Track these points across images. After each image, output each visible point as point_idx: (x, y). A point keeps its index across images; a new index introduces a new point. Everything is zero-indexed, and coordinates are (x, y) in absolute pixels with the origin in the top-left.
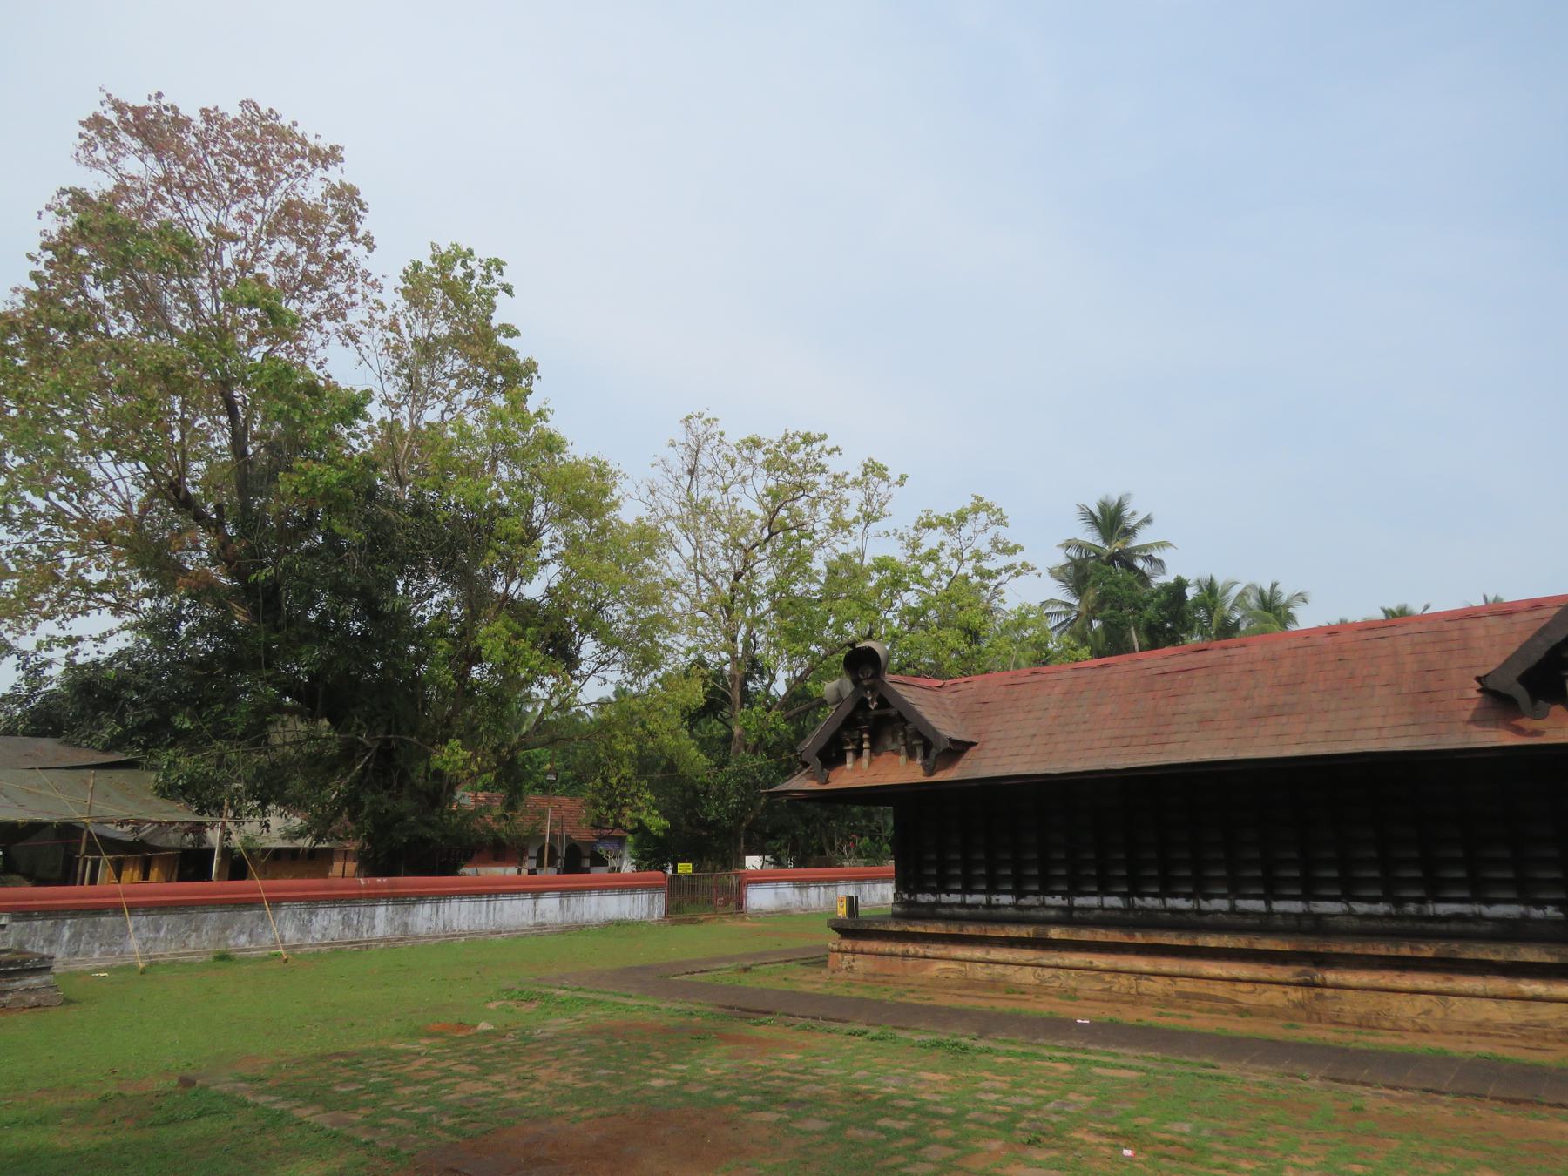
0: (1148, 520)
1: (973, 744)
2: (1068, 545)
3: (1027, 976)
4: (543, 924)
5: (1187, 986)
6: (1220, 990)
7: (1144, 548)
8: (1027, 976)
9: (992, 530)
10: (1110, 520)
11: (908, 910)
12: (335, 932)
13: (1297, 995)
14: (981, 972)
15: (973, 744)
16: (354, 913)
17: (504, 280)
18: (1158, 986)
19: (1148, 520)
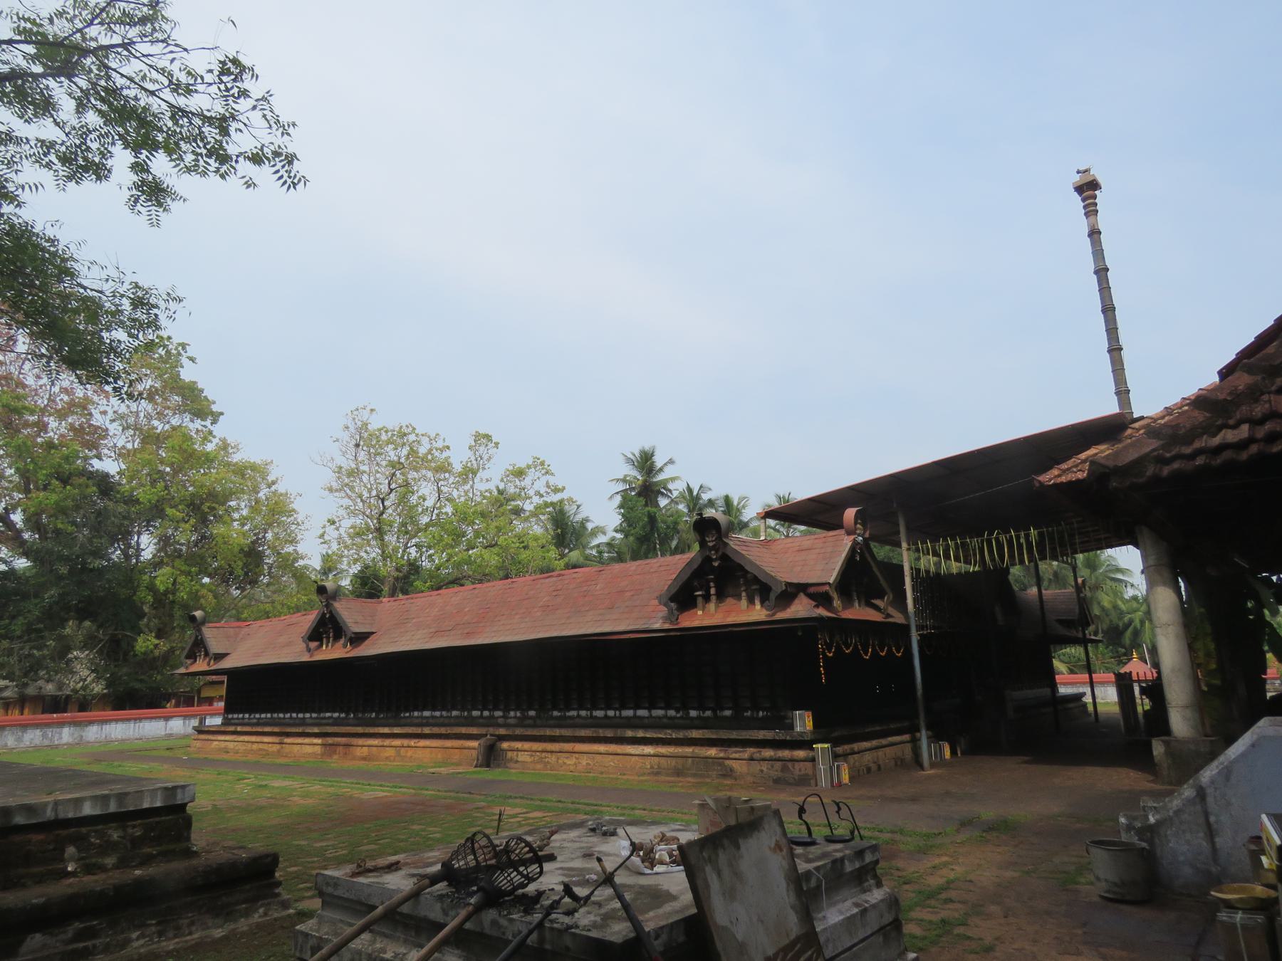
0: (671, 462)
1: (227, 654)
2: (624, 481)
3: (231, 745)
4: (171, 735)
5: (261, 746)
6: (265, 747)
7: (665, 481)
8: (231, 745)
9: (544, 479)
10: (645, 462)
11: (226, 722)
12: (37, 741)
13: (278, 747)
14: (223, 745)
15: (227, 654)
16: (49, 732)
17: (189, 354)
18: (255, 746)
19: (671, 462)
